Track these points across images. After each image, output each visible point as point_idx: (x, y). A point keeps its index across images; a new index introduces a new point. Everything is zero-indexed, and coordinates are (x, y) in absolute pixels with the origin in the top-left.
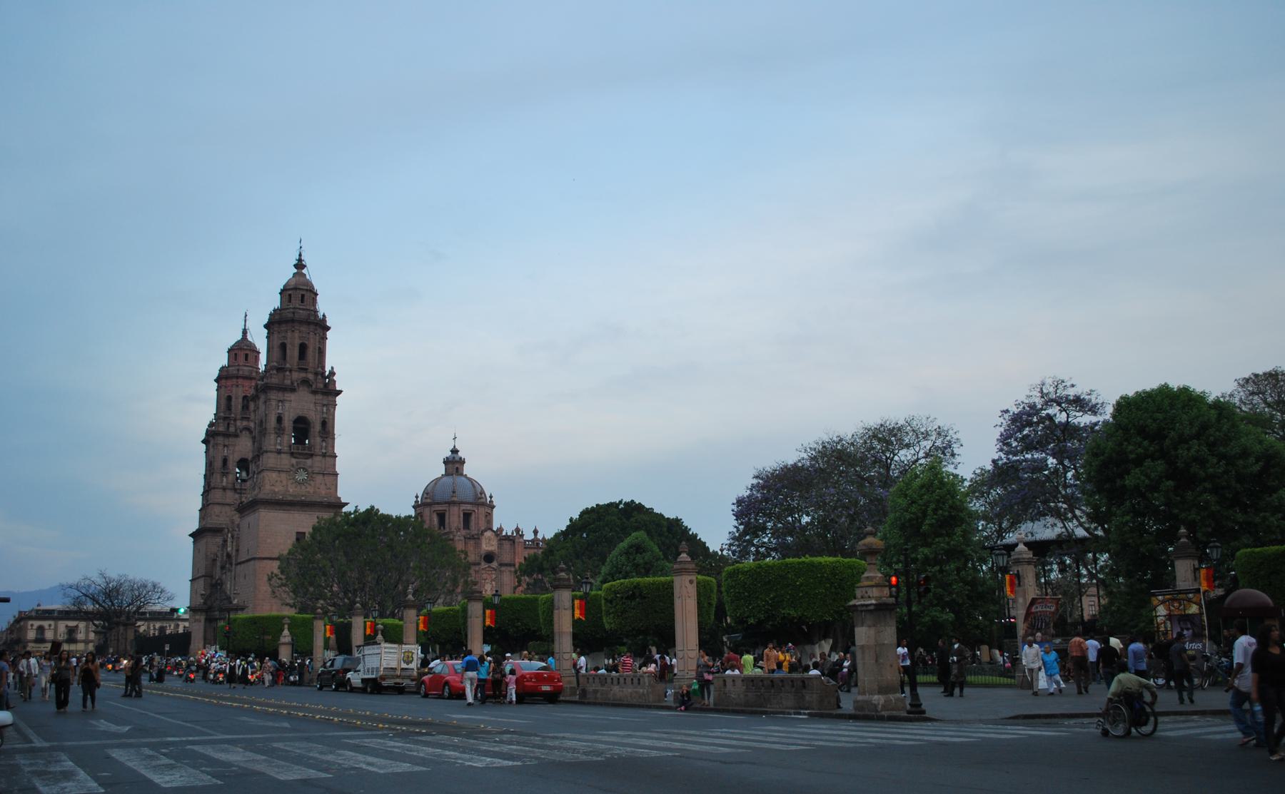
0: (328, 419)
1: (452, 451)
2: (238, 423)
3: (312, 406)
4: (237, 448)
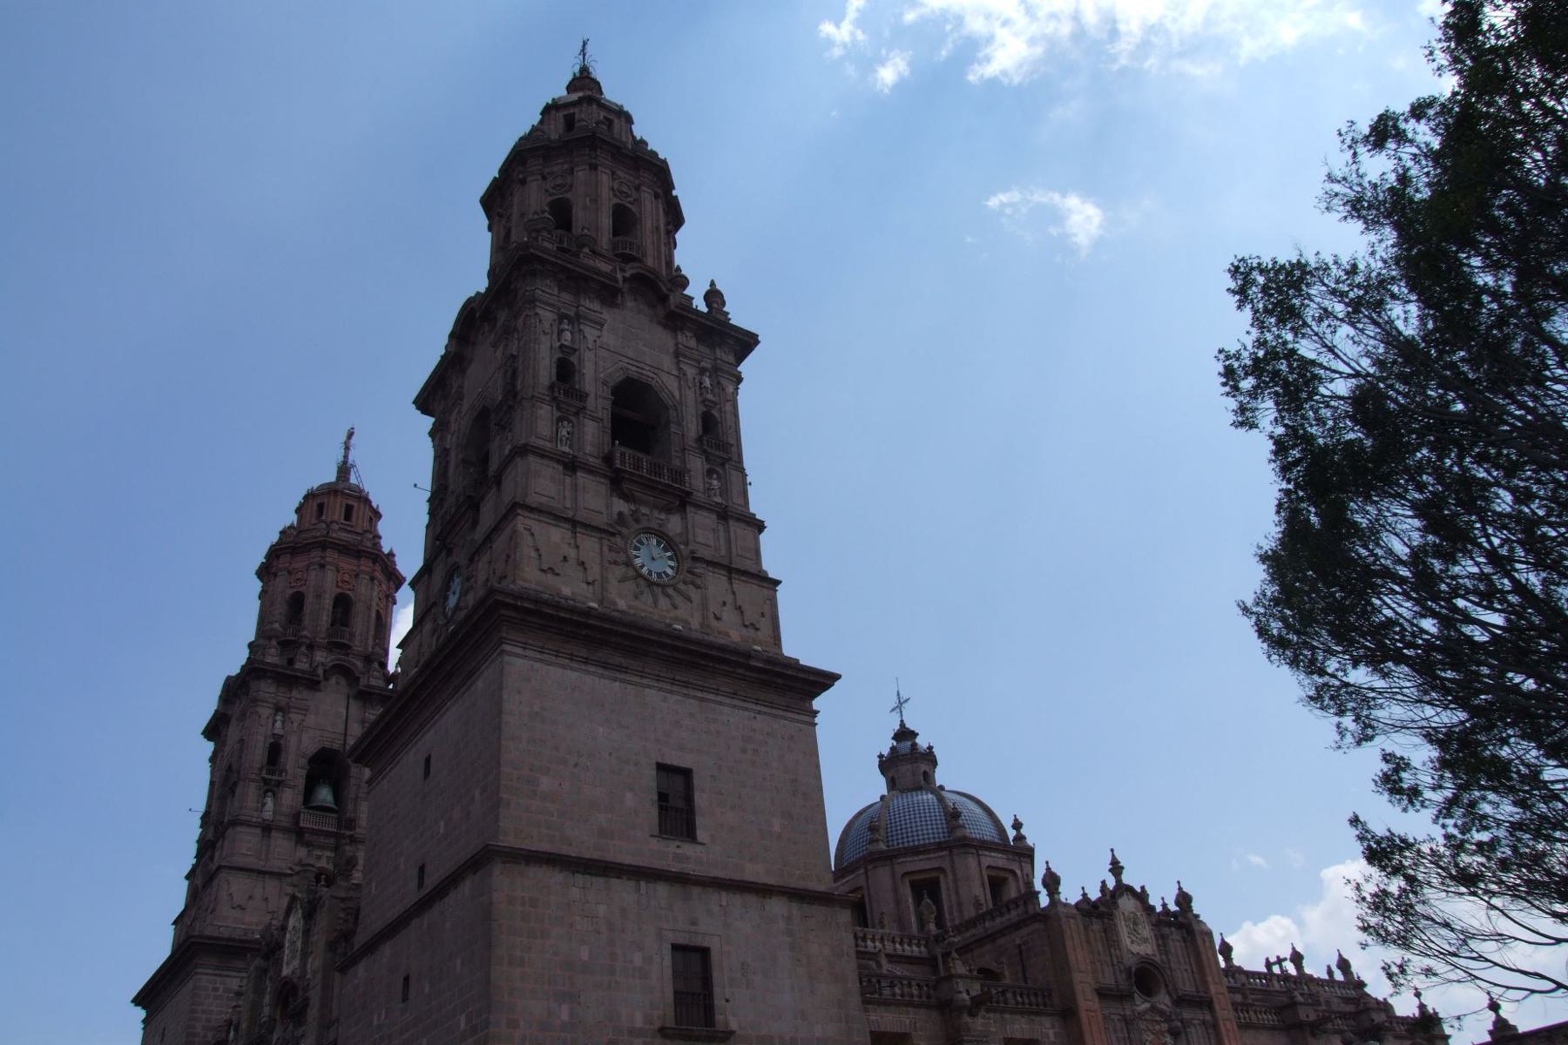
0: (720, 411)
1: (897, 737)
2: (320, 656)
3: (667, 363)
4: (311, 719)
